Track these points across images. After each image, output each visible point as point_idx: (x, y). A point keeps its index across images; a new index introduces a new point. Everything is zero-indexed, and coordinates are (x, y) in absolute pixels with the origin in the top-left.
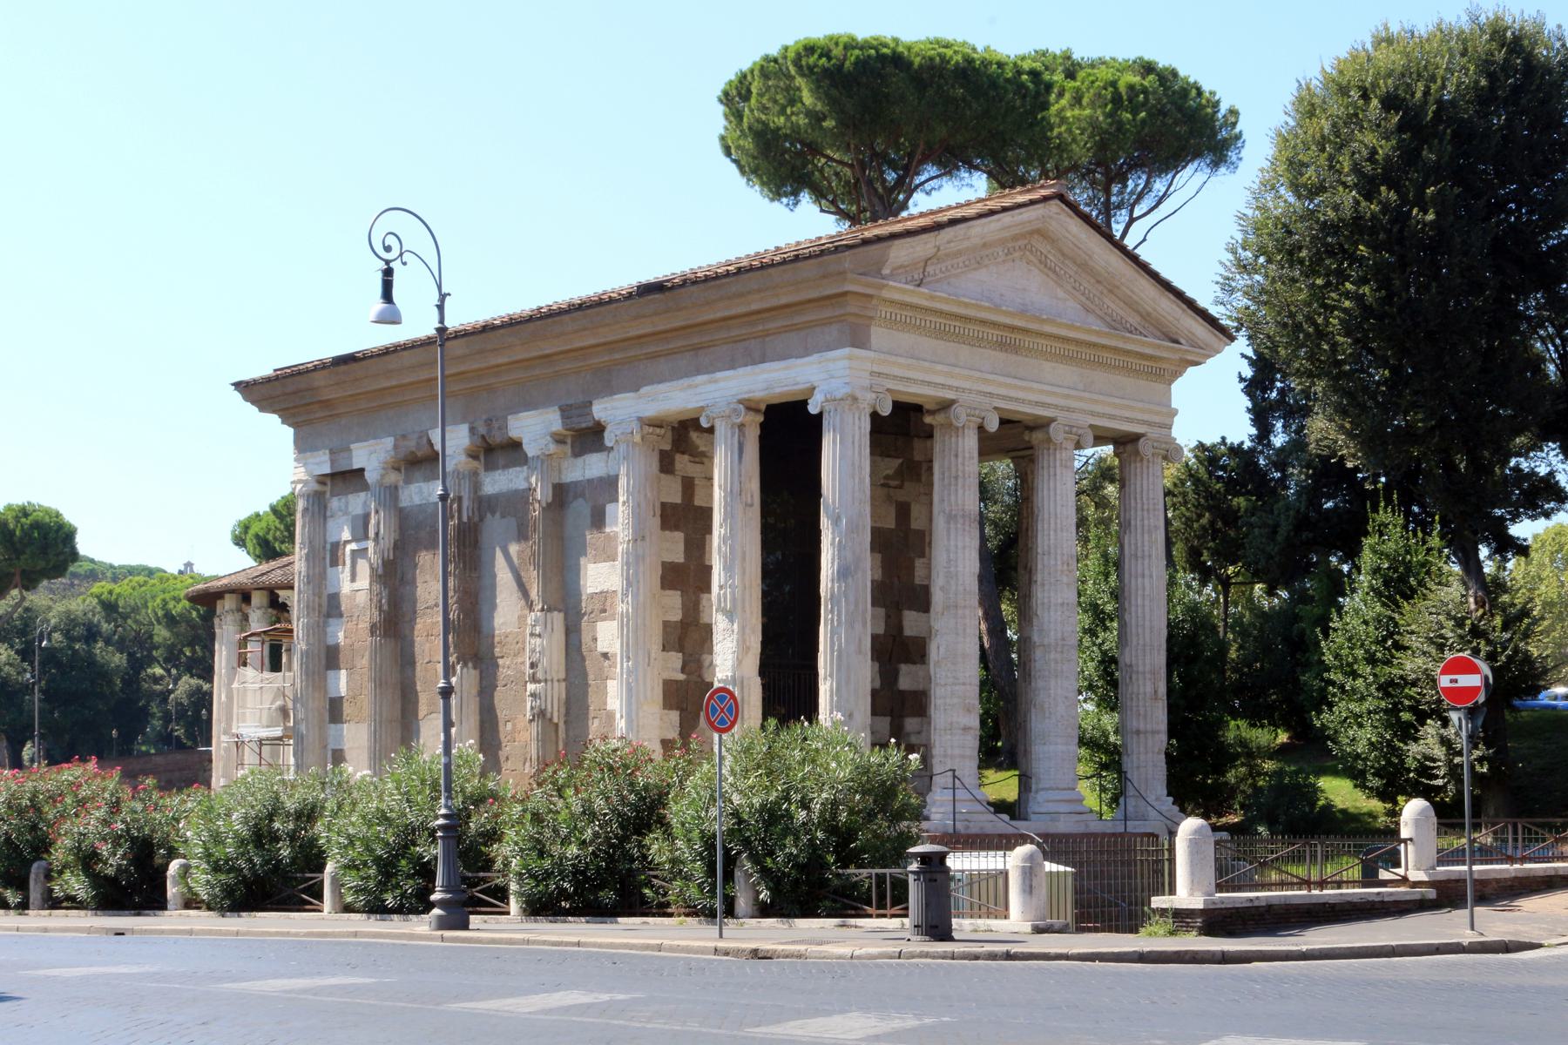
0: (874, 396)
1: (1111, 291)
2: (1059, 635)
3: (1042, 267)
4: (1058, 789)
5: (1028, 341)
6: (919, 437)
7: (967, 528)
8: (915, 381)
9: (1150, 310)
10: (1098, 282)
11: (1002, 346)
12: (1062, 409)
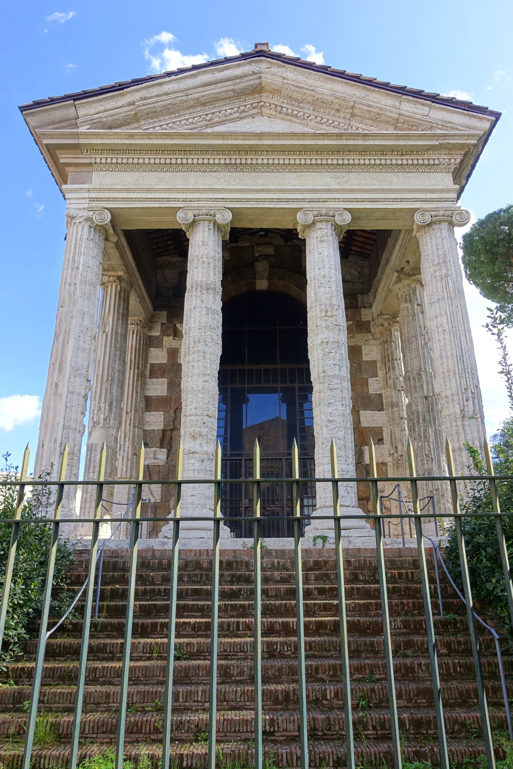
0: (91, 213)
1: (353, 115)
2: (321, 370)
3: (282, 116)
4: (326, 507)
6: (365, 307)
9: (396, 116)
10: (338, 111)
12: (311, 201)
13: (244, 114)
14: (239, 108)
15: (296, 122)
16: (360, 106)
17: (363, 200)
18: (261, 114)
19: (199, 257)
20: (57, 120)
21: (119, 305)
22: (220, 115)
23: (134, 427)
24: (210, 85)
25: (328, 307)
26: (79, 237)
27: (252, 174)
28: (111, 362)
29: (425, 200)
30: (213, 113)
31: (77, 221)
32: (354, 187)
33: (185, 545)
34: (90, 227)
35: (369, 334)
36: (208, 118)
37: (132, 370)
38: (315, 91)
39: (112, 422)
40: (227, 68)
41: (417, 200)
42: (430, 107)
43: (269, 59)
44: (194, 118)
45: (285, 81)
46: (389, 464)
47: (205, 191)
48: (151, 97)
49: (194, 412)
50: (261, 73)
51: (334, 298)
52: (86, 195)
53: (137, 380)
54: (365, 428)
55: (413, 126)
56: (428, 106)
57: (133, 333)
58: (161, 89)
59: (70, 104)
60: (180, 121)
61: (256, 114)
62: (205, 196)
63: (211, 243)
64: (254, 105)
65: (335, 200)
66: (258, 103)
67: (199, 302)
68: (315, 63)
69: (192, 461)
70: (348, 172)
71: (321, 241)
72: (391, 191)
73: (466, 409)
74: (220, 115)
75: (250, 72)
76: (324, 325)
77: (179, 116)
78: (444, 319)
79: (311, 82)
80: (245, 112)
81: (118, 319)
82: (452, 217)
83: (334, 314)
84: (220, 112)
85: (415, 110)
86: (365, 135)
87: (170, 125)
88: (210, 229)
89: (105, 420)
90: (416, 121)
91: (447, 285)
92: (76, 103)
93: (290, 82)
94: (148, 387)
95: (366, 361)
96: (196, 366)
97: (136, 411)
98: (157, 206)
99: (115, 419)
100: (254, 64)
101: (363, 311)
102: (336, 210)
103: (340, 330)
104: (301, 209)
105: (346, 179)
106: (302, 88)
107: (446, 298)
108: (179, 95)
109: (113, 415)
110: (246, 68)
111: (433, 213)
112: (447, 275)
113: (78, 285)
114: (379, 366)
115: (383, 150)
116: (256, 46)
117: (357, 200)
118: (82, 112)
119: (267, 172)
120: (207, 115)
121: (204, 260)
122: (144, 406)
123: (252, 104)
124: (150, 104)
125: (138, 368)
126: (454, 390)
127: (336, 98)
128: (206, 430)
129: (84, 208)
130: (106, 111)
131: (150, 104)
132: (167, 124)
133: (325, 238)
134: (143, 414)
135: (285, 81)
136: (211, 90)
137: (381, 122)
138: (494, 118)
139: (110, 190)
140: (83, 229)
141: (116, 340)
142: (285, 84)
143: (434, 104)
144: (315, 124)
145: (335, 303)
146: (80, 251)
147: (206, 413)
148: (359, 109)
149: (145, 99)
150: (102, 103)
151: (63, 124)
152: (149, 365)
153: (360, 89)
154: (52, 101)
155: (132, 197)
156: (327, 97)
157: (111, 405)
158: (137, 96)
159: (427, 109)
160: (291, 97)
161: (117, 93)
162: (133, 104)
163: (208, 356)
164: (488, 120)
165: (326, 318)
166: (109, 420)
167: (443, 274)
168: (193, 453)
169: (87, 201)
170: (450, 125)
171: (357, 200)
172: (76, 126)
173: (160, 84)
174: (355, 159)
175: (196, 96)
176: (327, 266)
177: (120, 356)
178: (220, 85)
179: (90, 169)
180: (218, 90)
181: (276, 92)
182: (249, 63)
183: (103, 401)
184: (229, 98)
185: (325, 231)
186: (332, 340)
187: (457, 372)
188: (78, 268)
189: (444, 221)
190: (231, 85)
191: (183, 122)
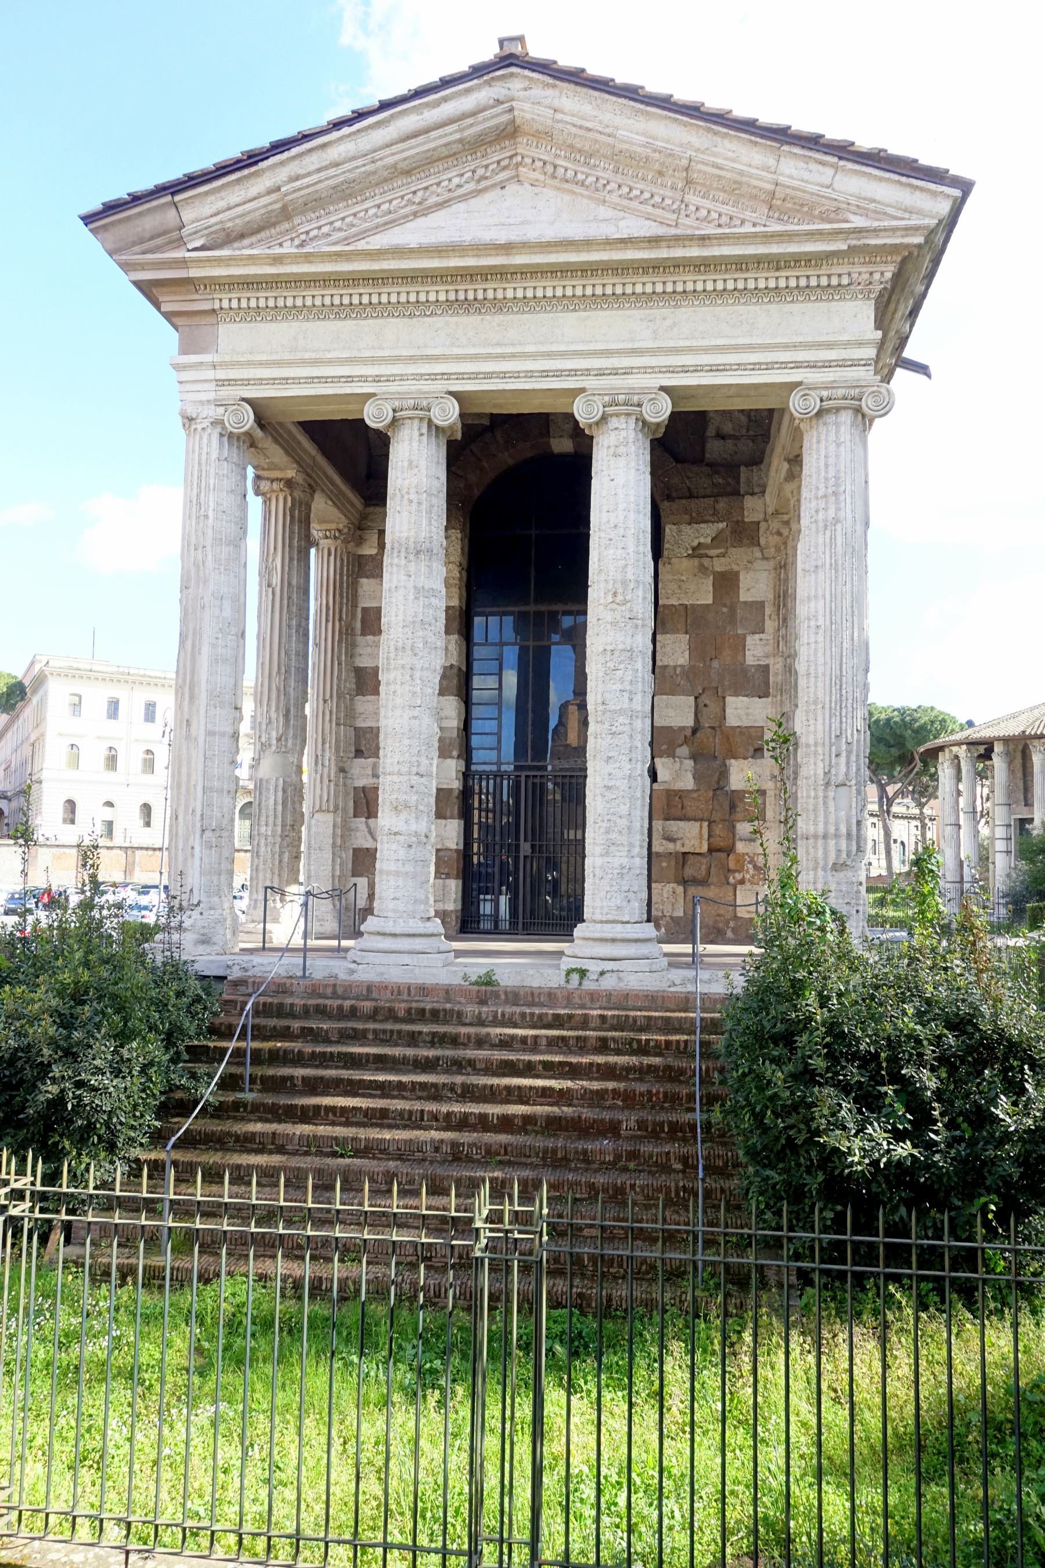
0: (221, 410)
2: (600, 700)
3: (556, 183)
5: (510, 290)
6: (753, 494)
7: (403, 562)
8: (297, 381)
9: (770, 187)
10: (661, 173)
11: (466, 306)
12: (601, 373)
13: (484, 184)
14: (474, 172)
15: (582, 195)
16: (700, 167)
17: (697, 369)
18: (517, 179)
19: (404, 492)
20: (147, 235)
21: (292, 532)
22: (439, 190)
23: (338, 724)
24: (416, 136)
25: (619, 585)
26: (204, 457)
27: (499, 318)
28: (284, 640)
29: (812, 365)
30: (426, 188)
31: (199, 427)
32: (682, 343)
33: (382, 974)
34: (221, 435)
35: (756, 549)
36: (417, 200)
37: (330, 624)
38: (615, 137)
39: (290, 742)
40: (445, 99)
41: (798, 365)
42: (836, 167)
43: (527, 72)
44: (390, 202)
45: (559, 116)
46: (769, 793)
47: (412, 359)
48: (309, 174)
49: (396, 768)
50: (513, 100)
51: (630, 568)
52: (210, 374)
53: (340, 641)
54: (733, 728)
55: (802, 205)
56: (832, 166)
57: (329, 555)
58: (324, 155)
59: (167, 203)
60: (366, 211)
61: (508, 180)
62: (412, 369)
63: (423, 463)
64: (503, 164)
65: (645, 370)
66: (511, 157)
67: (403, 578)
68: (613, 80)
69: (394, 846)
70: (675, 307)
71: (615, 455)
72: (751, 348)
73: (833, 771)
74: (439, 190)
75: (491, 102)
76: (609, 619)
77: (363, 201)
78: (821, 603)
79: (607, 117)
80: (485, 178)
81: (291, 559)
82: (860, 400)
83: (628, 598)
84: (438, 184)
85: (806, 175)
86: (703, 238)
87: (348, 220)
88: (421, 435)
89: (279, 740)
90: (807, 196)
91: (833, 539)
92: (177, 198)
93: (568, 119)
94: (360, 650)
95: (745, 603)
96: (399, 692)
97: (339, 696)
98: (330, 392)
99: (295, 737)
100: (498, 84)
101: (749, 502)
102: (644, 390)
103: (637, 626)
104: (583, 390)
105: (668, 322)
106: (589, 130)
107: (828, 566)
108: (359, 162)
109: (291, 732)
110: (482, 94)
111: (825, 394)
112: (837, 521)
113: (208, 548)
114: (768, 611)
115: (740, 264)
116: (501, 42)
117: (685, 370)
118: (188, 215)
119: (524, 312)
120: (415, 193)
121: (412, 497)
122: (354, 686)
123: (498, 162)
124: (308, 187)
125: (340, 619)
126: (820, 735)
127: (655, 151)
128: (415, 798)
129: (209, 401)
130: (229, 208)
131: (308, 187)
132: (343, 219)
133: (622, 450)
134: (352, 700)
135: (559, 116)
136: (418, 145)
137: (741, 195)
138: (957, 193)
139: (250, 364)
140: (209, 441)
141: (289, 598)
142: (558, 121)
143: (842, 163)
144: (617, 200)
145: (632, 577)
146: (207, 485)
147: (414, 770)
148: (700, 171)
149: (297, 178)
150: (223, 194)
151: (159, 241)
152: (359, 610)
153: (701, 131)
154: (136, 199)
155: (286, 375)
156: (639, 149)
157: (287, 716)
158: (283, 174)
159: (830, 172)
160: (571, 146)
161: (246, 172)
162: (278, 189)
163: (418, 674)
164: (948, 196)
165: (614, 606)
166: (286, 740)
167: (830, 518)
168: (396, 834)
169: (212, 386)
170: (872, 206)
171: (685, 370)
172: (180, 242)
173: (324, 146)
174: (689, 281)
175: (391, 160)
176: (621, 506)
177: (299, 626)
178: (434, 134)
179: (211, 319)
180: (432, 145)
181: (544, 135)
182: (488, 83)
183: (273, 709)
184: (455, 154)
185: (624, 433)
186: (621, 647)
187: (827, 706)
188: (206, 517)
189: (845, 408)
190: (456, 131)
191: (371, 212)
